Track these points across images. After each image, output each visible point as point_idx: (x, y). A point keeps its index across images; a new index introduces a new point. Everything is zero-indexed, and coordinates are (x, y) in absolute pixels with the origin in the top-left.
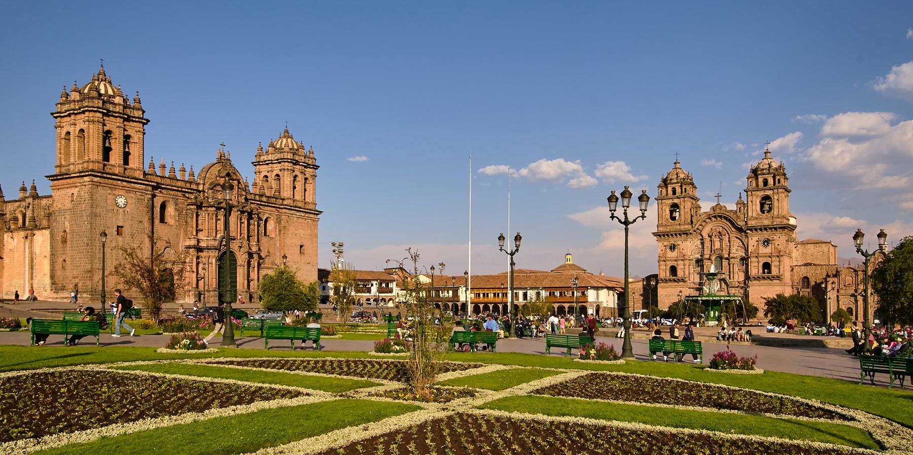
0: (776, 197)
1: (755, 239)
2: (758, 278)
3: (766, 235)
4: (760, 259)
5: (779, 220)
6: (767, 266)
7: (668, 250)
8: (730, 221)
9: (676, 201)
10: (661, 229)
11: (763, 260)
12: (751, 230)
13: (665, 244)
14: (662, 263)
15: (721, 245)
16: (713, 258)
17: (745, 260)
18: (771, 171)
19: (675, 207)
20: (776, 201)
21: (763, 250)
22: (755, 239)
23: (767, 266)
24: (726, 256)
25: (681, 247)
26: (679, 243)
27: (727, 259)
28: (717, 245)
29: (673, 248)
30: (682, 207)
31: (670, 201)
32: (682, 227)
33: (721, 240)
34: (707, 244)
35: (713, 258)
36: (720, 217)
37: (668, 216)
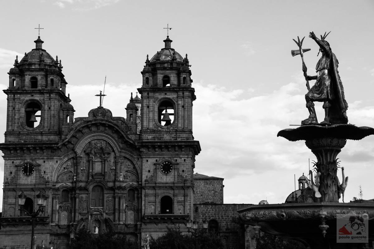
0: (180, 102)
1: (152, 161)
2: (154, 220)
3: (167, 156)
4: (159, 192)
5: (185, 135)
6: (167, 203)
7: (21, 174)
8: (117, 132)
9: (37, 97)
10: (12, 139)
11: (161, 193)
12: (147, 147)
13: (17, 162)
14: (10, 193)
15: (103, 168)
16: (91, 188)
17: (136, 192)
18: (175, 65)
19: (33, 106)
20: (180, 107)
21: (164, 179)
22: (152, 161)
23: (167, 203)
24: (110, 185)
25: (43, 169)
26: (40, 162)
27: (112, 189)
28: (98, 168)
29: (28, 170)
30: (46, 107)
31: (28, 98)
32: (45, 138)
33: (103, 161)
34: (83, 165)
35: (91, 188)
36: (104, 125)
37: (23, 120)
